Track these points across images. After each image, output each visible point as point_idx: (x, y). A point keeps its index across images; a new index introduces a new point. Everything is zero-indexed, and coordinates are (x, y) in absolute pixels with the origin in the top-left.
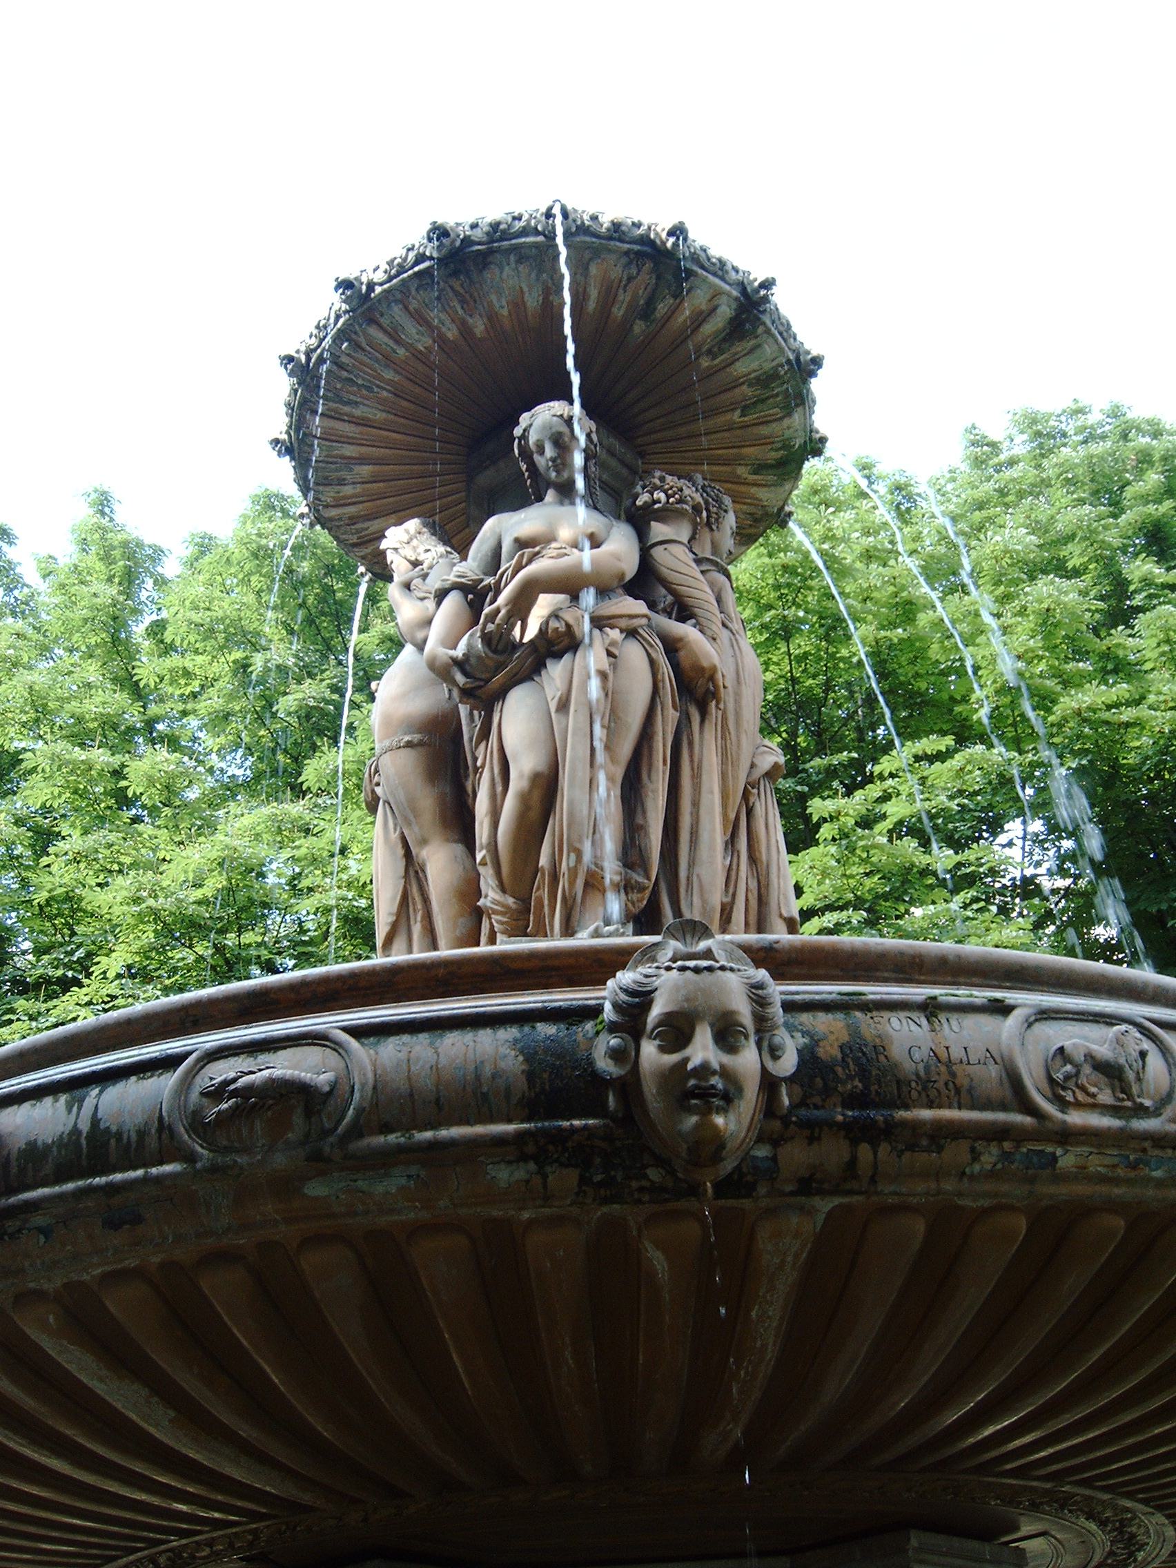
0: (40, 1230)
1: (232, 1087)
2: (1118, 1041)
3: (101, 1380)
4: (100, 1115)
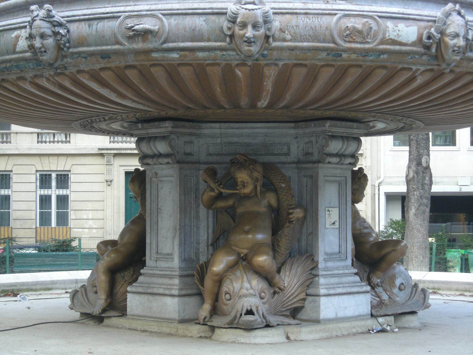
0: (84, 57)
1: (133, 29)
2: (364, 24)
3: (98, 88)
4: (98, 30)
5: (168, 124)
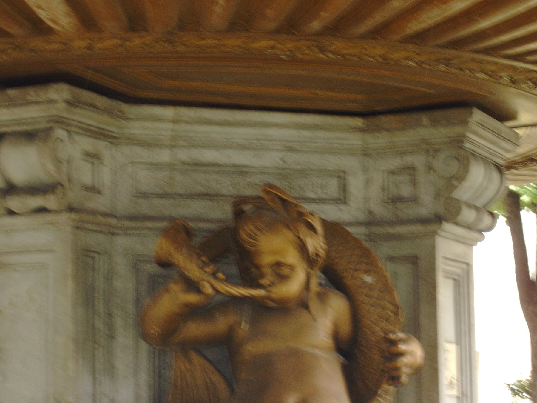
5: (60, 93)
